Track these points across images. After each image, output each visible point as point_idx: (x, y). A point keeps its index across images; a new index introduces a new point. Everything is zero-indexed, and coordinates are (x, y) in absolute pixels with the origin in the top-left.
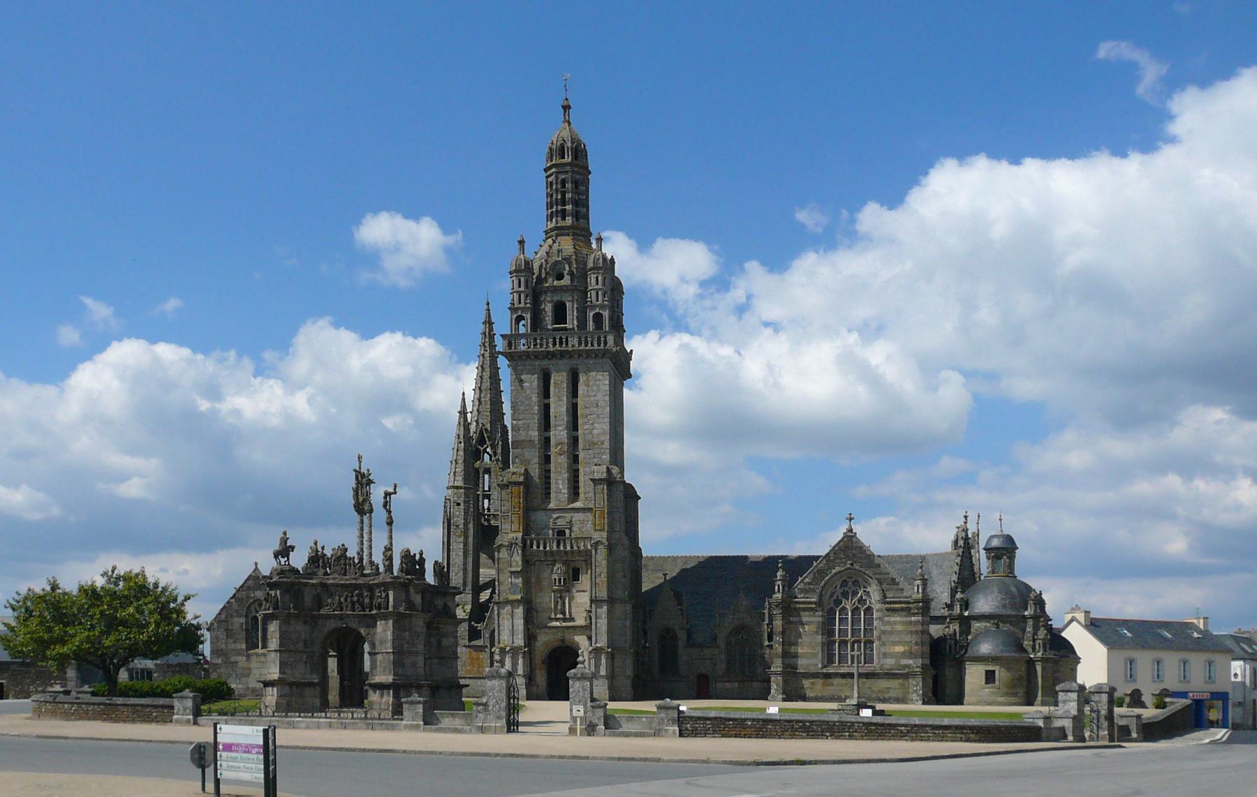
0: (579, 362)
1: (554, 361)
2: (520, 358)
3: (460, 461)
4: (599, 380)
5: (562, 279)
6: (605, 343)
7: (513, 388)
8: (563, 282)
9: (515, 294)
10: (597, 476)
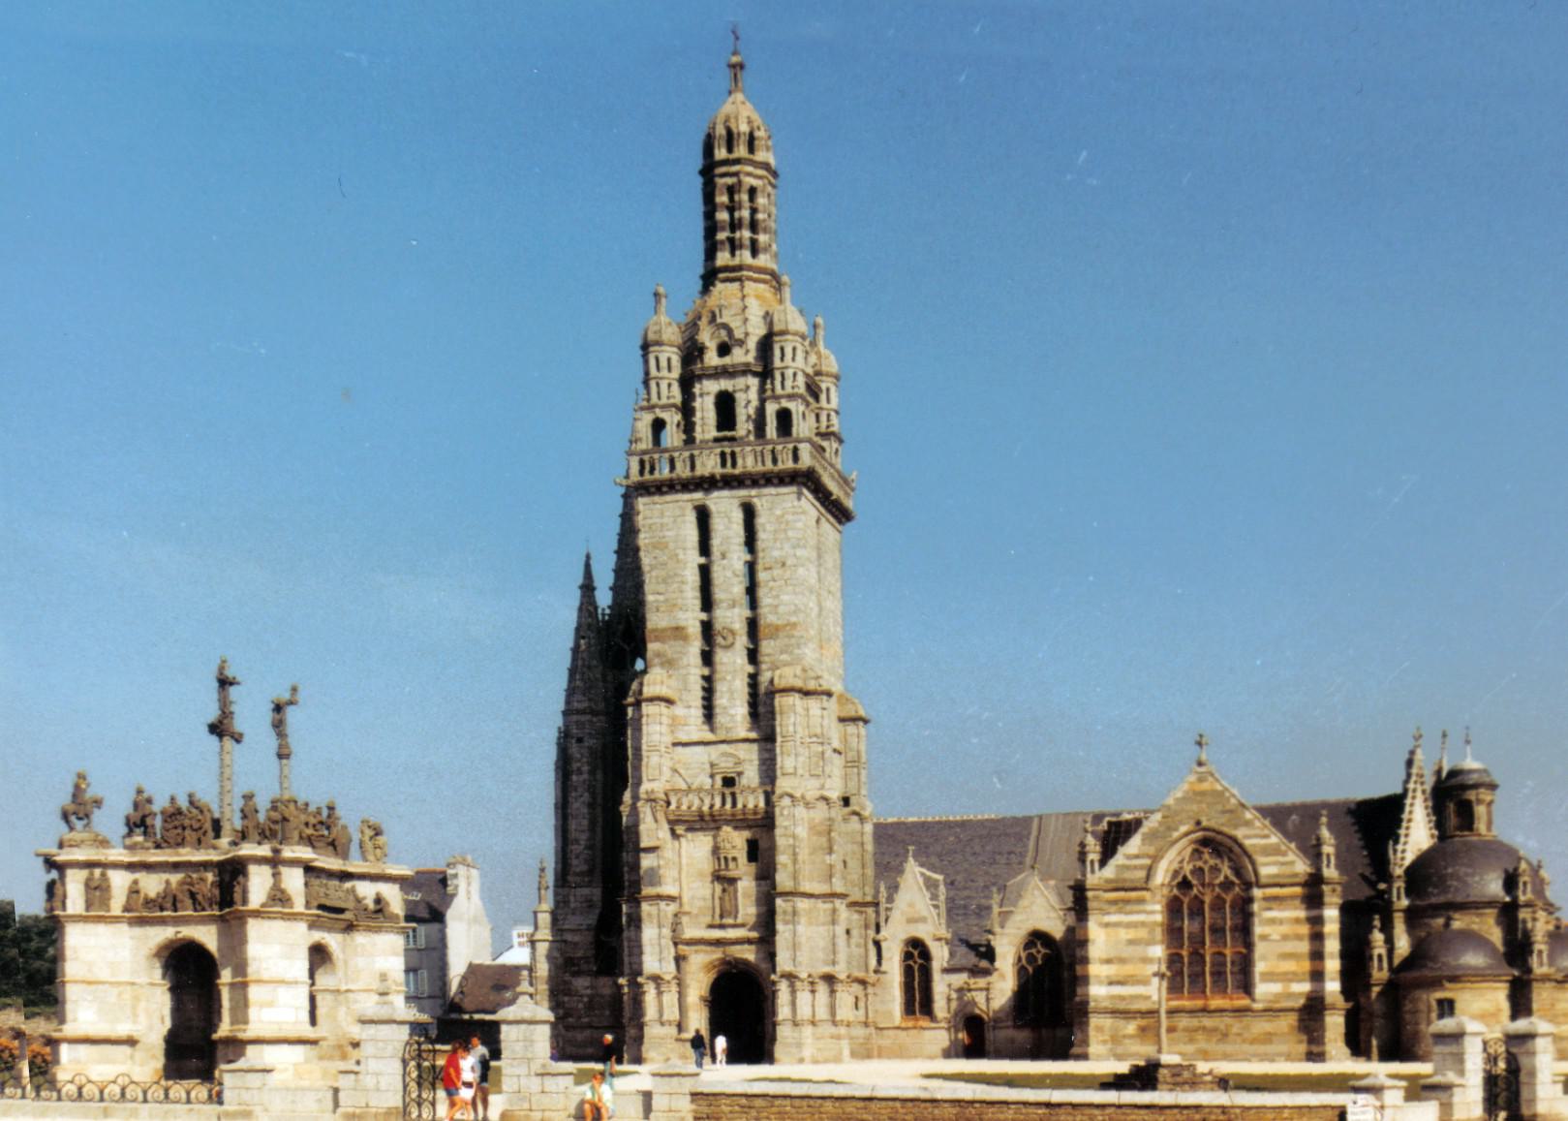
0: (754, 492)
6: (796, 458)
8: (727, 360)
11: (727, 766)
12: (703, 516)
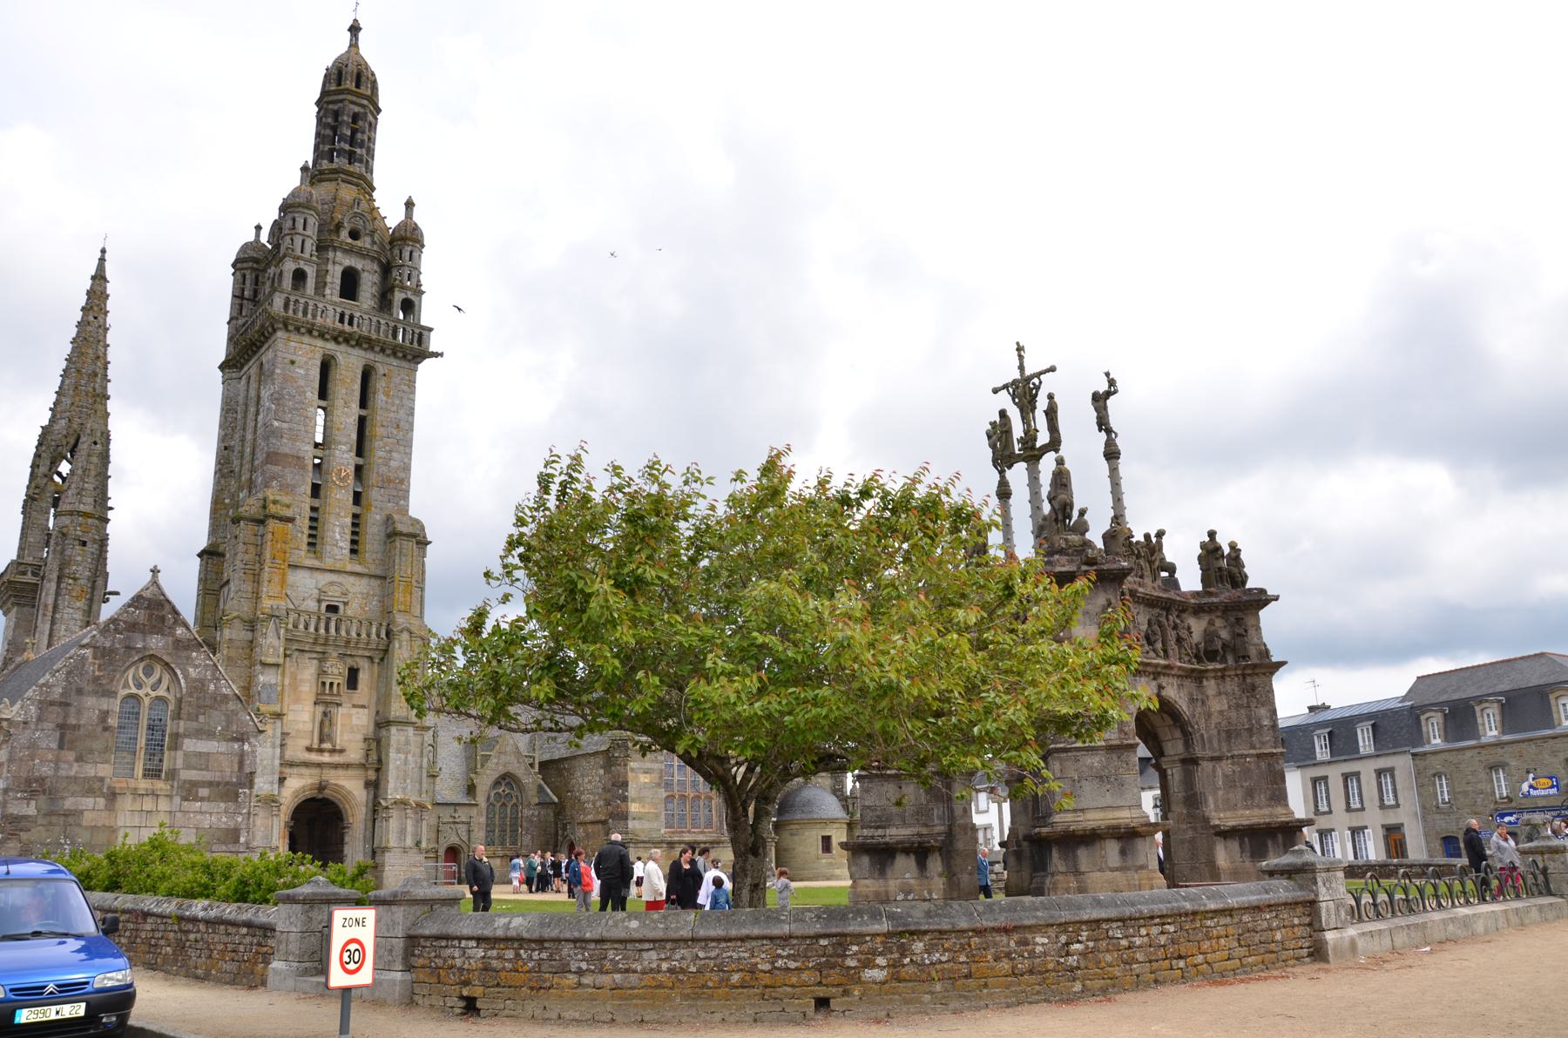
0: (379, 357)
1: (343, 347)
2: (297, 329)
3: (93, 473)
8: (359, 243)
11: (334, 596)
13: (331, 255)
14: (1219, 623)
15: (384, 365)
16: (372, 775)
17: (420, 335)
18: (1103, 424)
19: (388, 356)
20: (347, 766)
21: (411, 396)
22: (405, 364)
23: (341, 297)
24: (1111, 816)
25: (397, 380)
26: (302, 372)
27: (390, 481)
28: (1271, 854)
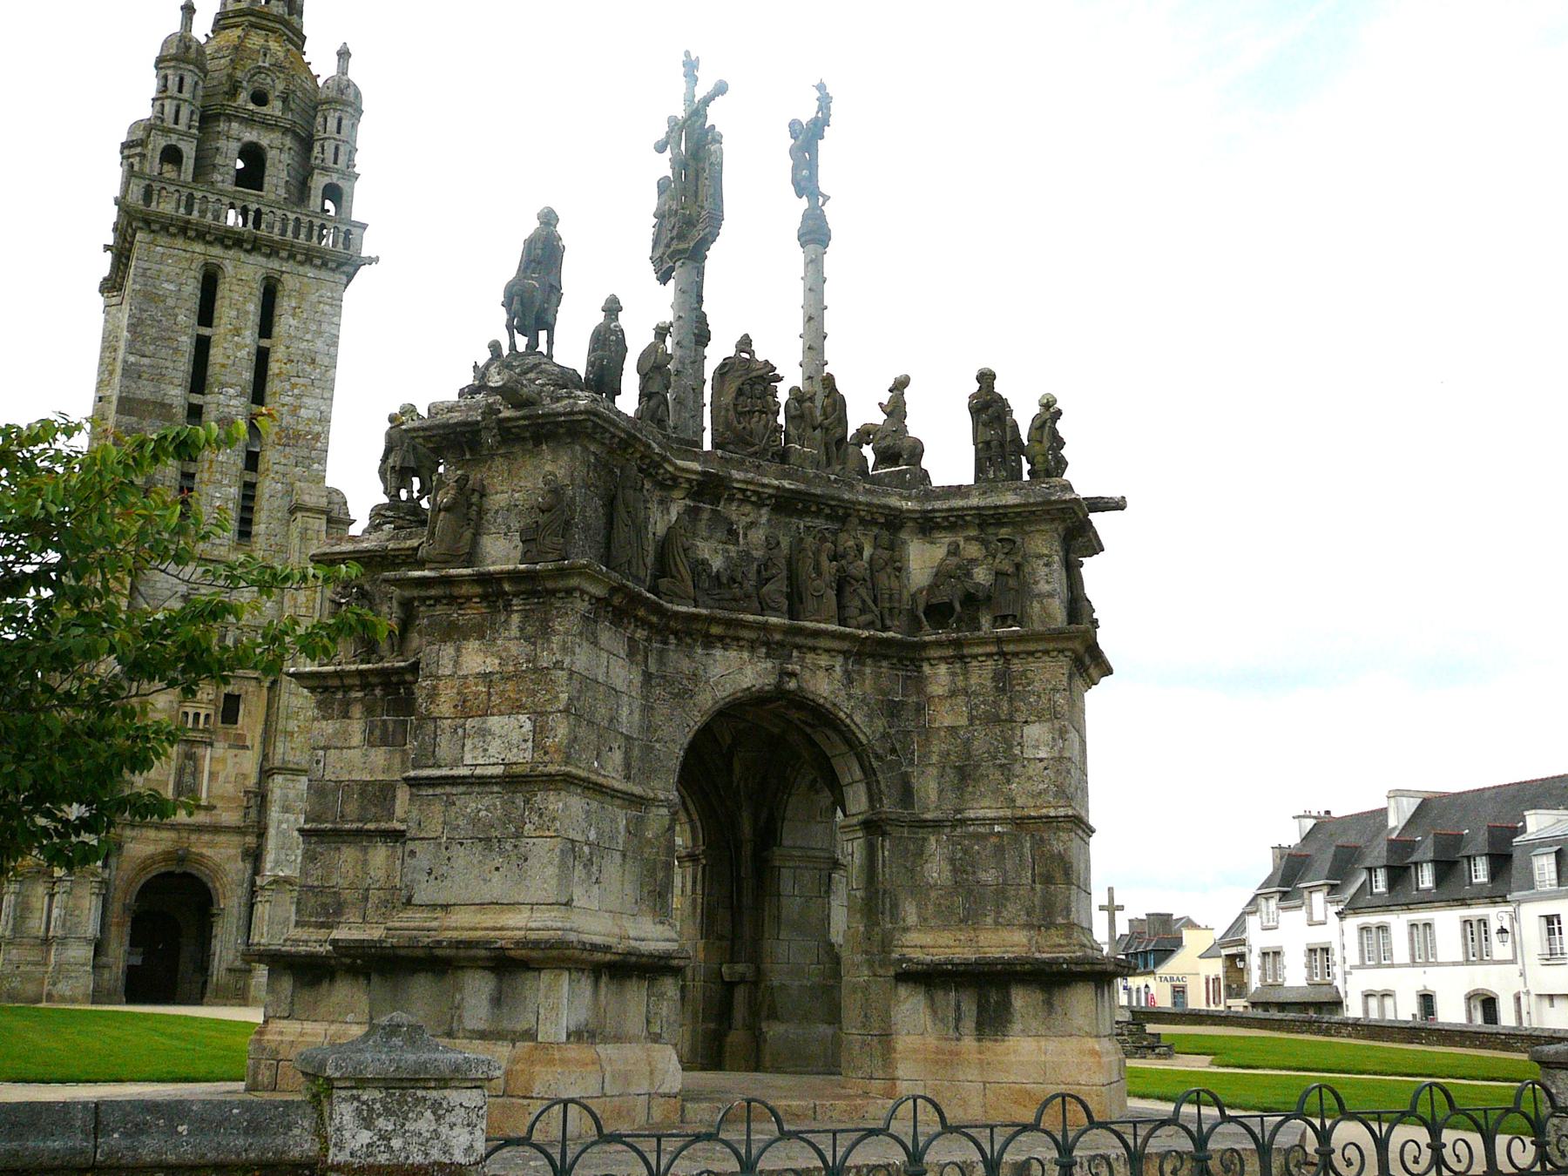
2: (165, 228)
4: (323, 313)
5: (265, 105)
7: (137, 287)
8: (264, 110)
9: (167, 102)
10: (309, 500)
12: (210, 283)
13: (223, 126)
14: (973, 550)
15: (294, 278)
16: (251, 840)
17: (348, 233)
18: (805, 182)
19: (301, 263)
20: (216, 829)
21: (335, 319)
22: (324, 274)
23: (237, 185)
24: (490, 924)
25: (314, 298)
26: (172, 287)
27: (298, 436)
28: (1017, 1027)
